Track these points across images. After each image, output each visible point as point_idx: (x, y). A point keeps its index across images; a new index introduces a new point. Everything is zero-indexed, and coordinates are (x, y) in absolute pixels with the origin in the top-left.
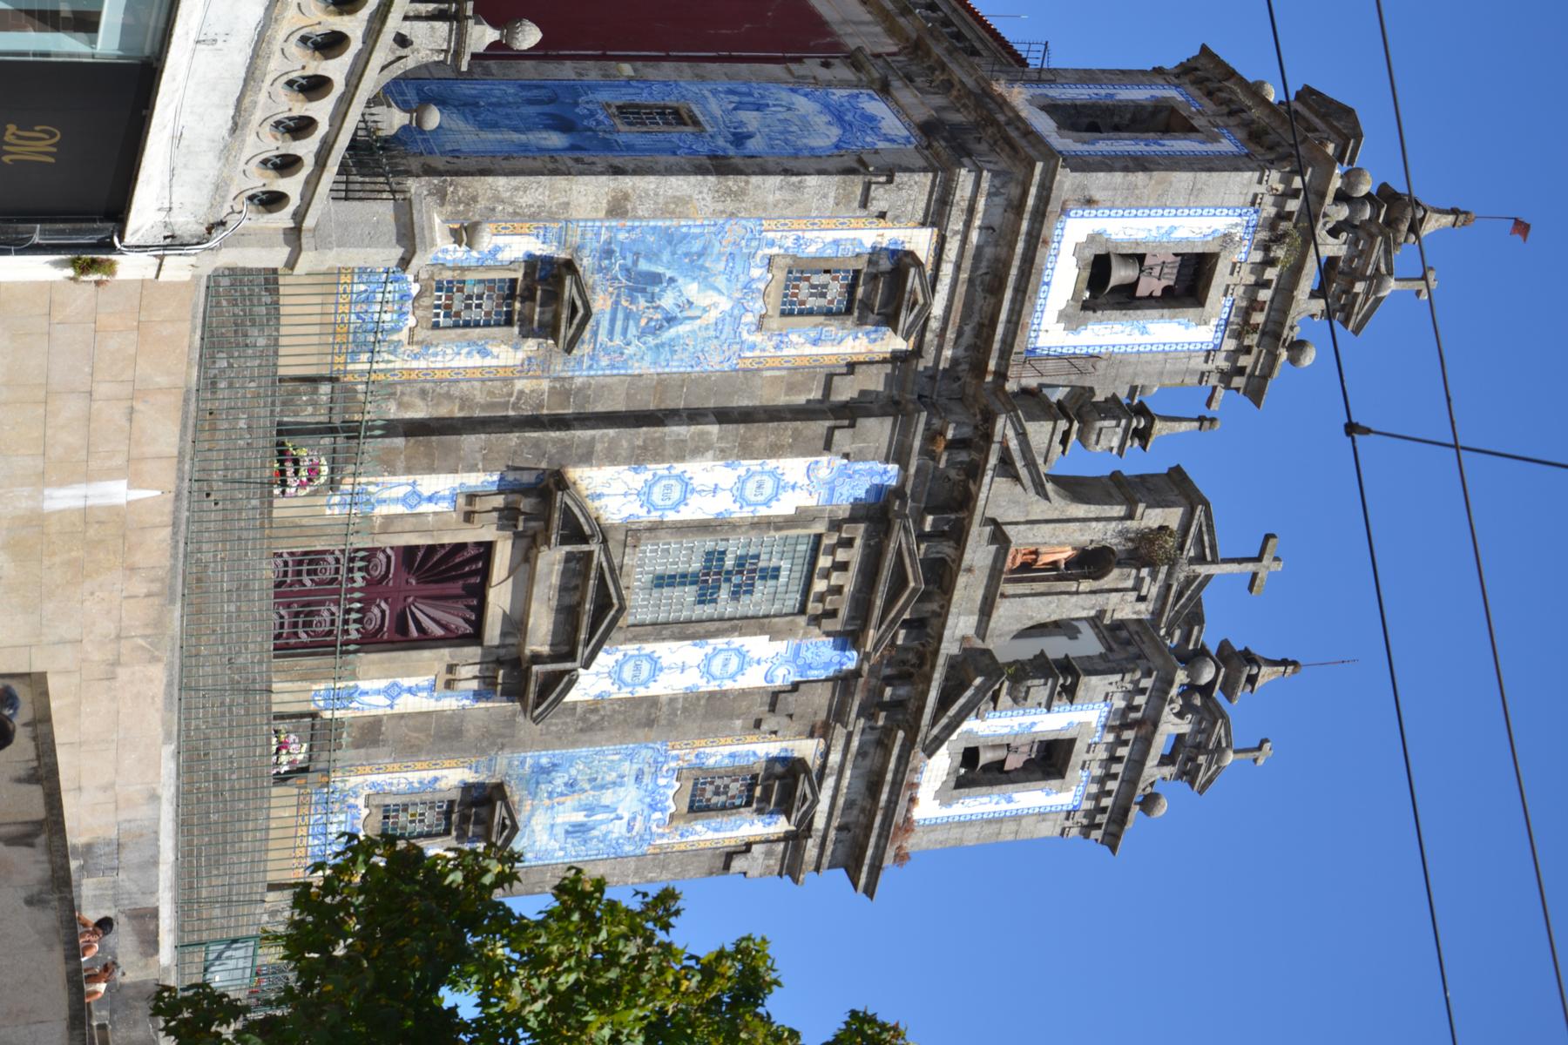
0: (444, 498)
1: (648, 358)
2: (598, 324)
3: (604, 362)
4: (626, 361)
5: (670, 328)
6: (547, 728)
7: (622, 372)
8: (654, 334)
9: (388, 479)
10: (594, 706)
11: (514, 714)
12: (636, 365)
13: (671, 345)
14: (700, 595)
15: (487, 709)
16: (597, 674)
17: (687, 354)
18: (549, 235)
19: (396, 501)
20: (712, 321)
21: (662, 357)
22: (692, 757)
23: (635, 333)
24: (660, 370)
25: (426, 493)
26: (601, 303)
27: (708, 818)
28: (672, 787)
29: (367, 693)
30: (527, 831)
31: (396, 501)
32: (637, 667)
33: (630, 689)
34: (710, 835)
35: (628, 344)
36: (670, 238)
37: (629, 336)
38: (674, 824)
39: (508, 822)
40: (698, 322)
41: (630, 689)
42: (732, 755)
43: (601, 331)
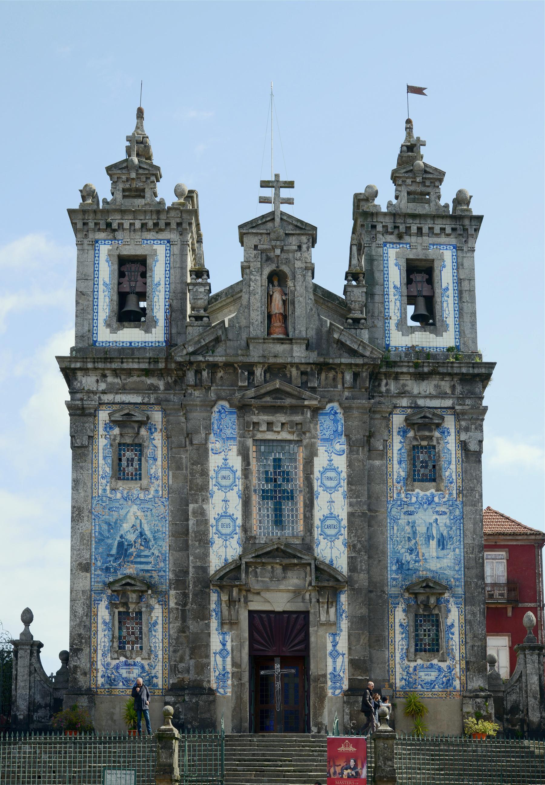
0: (224, 639)
1: (160, 543)
2: (142, 570)
3: (162, 565)
4: (162, 554)
5: (145, 534)
6: (363, 571)
7: (167, 555)
8: (148, 542)
9: (212, 667)
10: (351, 547)
11: (353, 589)
12: (164, 548)
13: (154, 532)
14: (288, 499)
15: (349, 604)
16: (331, 548)
17: (160, 525)
18: (98, 598)
19: (224, 661)
20: (142, 514)
21: (161, 536)
22: (399, 486)
23: (147, 551)
24: (167, 537)
25: (221, 647)
26: (130, 570)
27: (440, 469)
28: (418, 493)
29: (335, 668)
30: (439, 571)
31: (224, 661)
32: (329, 527)
33: (342, 529)
34: (453, 467)
35: (153, 554)
36: (101, 540)
37: (149, 554)
38: (443, 488)
39: (424, 585)
40: (142, 521)
41: (342, 529)
42: (400, 463)
43: (146, 568)
